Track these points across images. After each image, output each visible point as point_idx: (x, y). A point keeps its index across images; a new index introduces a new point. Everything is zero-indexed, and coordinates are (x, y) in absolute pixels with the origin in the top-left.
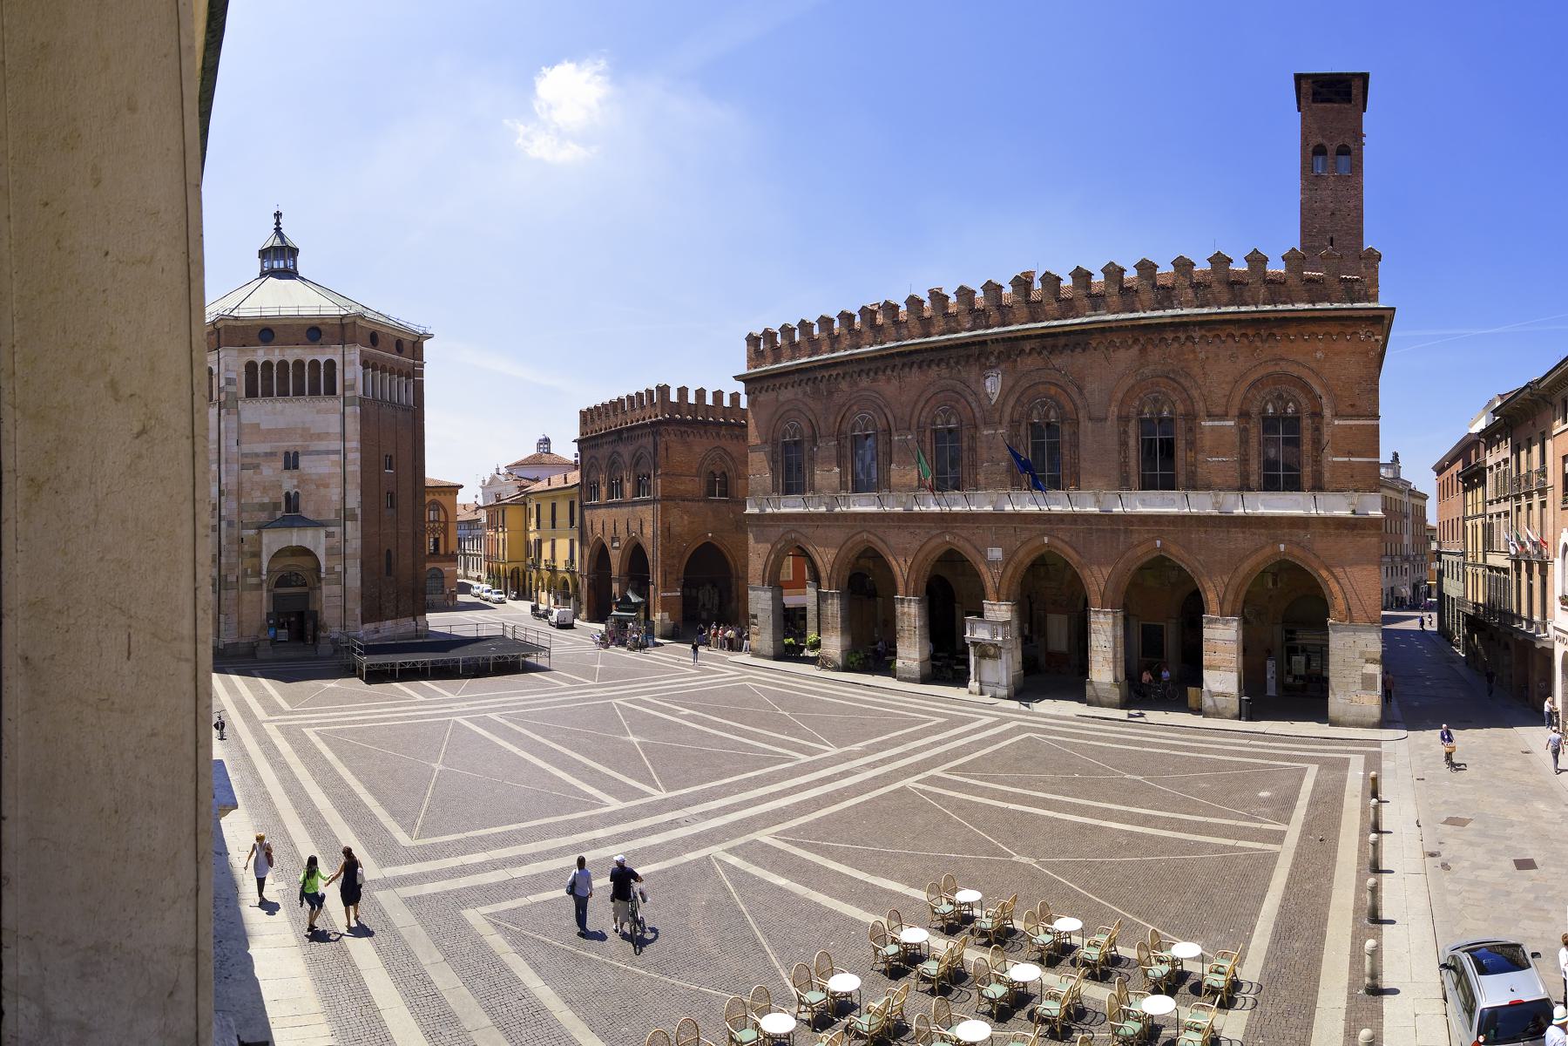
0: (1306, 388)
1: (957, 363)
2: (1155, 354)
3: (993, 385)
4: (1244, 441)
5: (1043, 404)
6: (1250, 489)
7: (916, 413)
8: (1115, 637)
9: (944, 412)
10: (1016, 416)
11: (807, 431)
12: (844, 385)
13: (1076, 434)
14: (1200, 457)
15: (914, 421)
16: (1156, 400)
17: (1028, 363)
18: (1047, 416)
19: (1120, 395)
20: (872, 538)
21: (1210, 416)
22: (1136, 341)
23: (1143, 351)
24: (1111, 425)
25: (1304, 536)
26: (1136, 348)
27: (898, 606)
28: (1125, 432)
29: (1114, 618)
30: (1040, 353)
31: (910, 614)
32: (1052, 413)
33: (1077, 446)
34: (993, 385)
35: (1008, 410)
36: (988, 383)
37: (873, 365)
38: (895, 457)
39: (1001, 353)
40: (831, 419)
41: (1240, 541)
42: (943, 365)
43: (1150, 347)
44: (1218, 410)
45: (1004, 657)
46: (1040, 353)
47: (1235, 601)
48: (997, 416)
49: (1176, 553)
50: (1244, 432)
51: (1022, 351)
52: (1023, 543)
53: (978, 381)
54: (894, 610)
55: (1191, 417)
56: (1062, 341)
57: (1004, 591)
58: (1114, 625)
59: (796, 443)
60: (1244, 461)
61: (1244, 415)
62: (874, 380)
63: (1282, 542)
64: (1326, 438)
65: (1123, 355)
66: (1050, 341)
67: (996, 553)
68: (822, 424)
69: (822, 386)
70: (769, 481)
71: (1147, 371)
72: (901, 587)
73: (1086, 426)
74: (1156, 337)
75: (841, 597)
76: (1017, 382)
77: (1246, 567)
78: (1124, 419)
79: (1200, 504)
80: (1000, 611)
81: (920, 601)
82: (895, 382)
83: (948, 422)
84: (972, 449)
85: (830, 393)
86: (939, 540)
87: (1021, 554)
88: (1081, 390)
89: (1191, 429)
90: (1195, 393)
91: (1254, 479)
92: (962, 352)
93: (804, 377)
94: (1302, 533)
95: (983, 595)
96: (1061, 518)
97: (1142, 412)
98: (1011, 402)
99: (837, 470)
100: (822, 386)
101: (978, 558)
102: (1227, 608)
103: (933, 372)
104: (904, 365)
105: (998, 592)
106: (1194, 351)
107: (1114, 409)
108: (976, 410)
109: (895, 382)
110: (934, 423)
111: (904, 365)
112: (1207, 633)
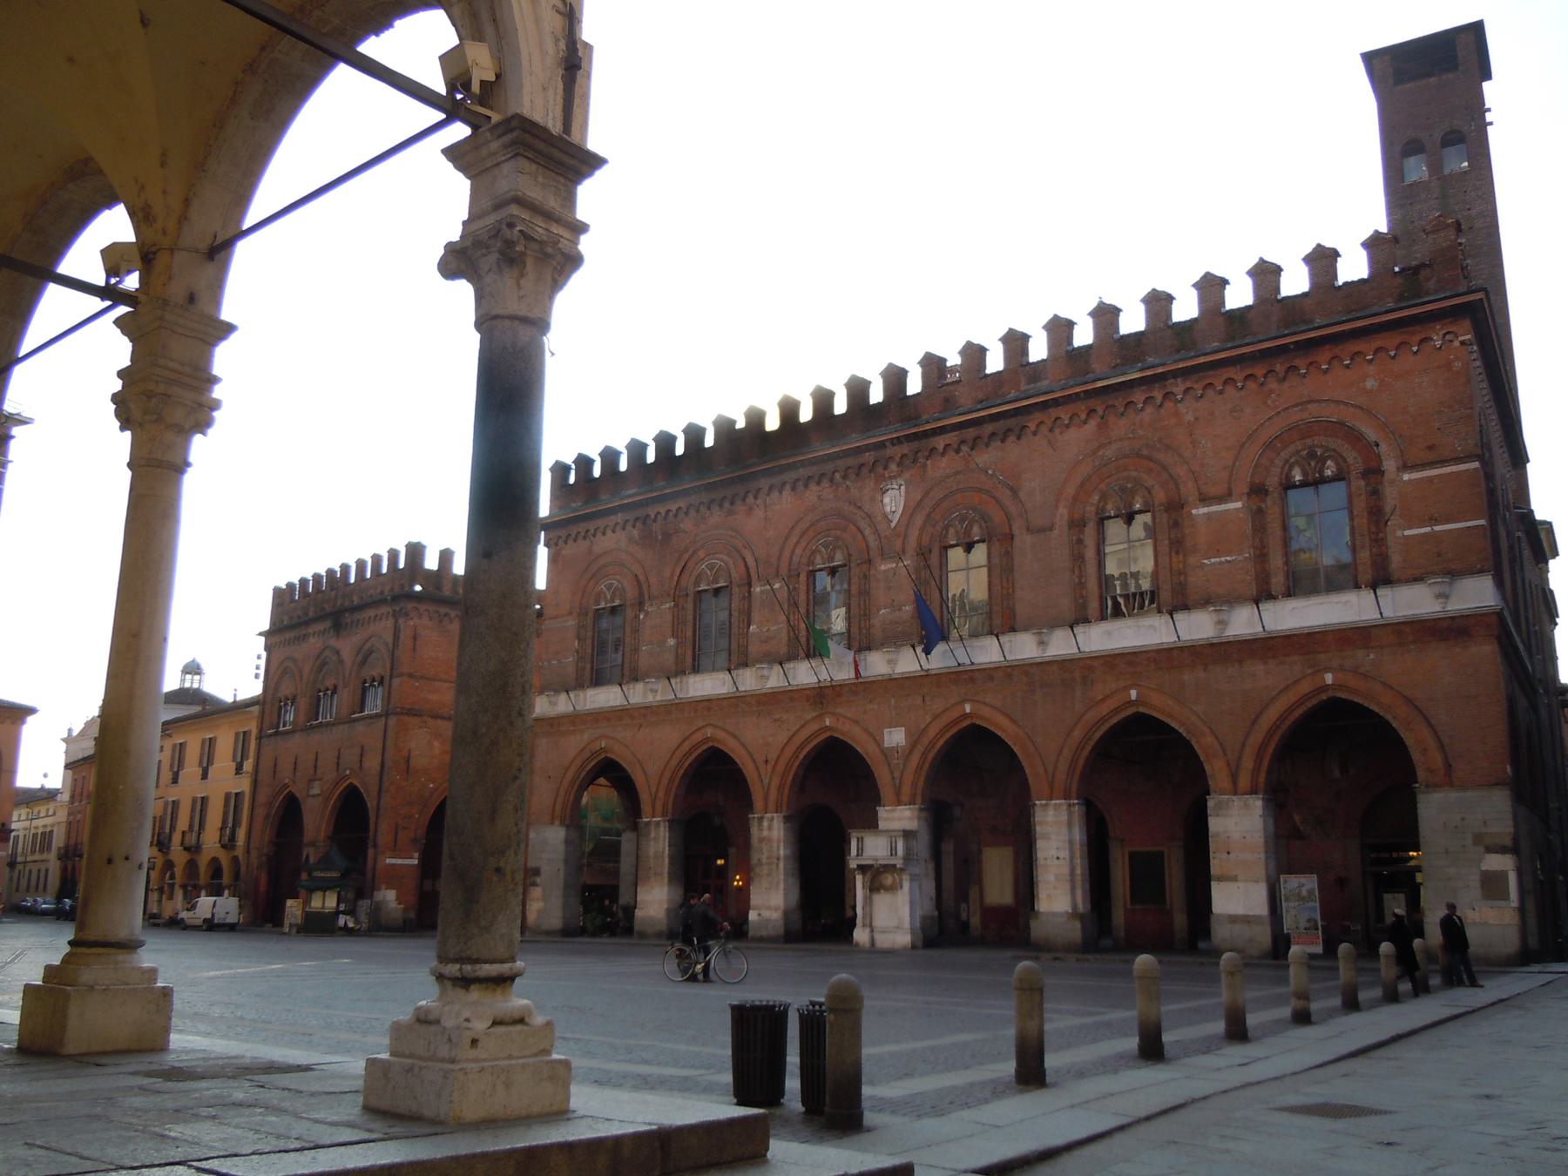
0: (1355, 437)
1: (845, 477)
2: (1120, 426)
3: (893, 501)
4: (1260, 528)
5: (962, 519)
6: (1271, 597)
7: (787, 554)
8: (1071, 842)
9: (826, 546)
10: (926, 540)
11: (631, 593)
13: (1008, 554)
14: (1192, 560)
16: (1123, 489)
17: (942, 466)
18: (968, 532)
19: (1070, 490)
20: (721, 735)
21: (1205, 499)
22: (1091, 412)
23: (1103, 425)
25: (1366, 658)
26: (1092, 425)
27: (754, 831)
28: (1080, 541)
29: (1070, 813)
30: (958, 451)
31: (771, 835)
32: (976, 529)
33: (1012, 570)
34: (893, 501)
35: (914, 534)
36: (887, 500)
38: (756, 616)
39: (903, 456)
41: (1262, 676)
42: (825, 483)
43: (1111, 419)
44: (1212, 490)
45: (906, 885)
46: (958, 451)
47: (1256, 769)
48: (899, 542)
49: (1163, 706)
50: (1259, 514)
51: (933, 449)
52: (935, 717)
53: (873, 499)
55: (1176, 506)
56: (989, 428)
57: (906, 790)
58: (1070, 825)
59: (614, 610)
60: (1261, 556)
61: (1257, 491)
62: (731, 513)
63: (1327, 670)
64: (1388, 509)
65: (1073, 434)
66: (971, 433)
67: (896, 737)
68: (653, 580)
70: (571, 670)
71: (1109, 453)
72: (758, 803)
73: (1024, 541)
74: (1119, 403)
75: (672, 823)
76: (926, 494)
77: (1272, 714)
78: (1077, 524)
79: (1197, 626)
80: (899, 817)
81: (787, 819)
82: (759, 513)
83: (832, 559)
85: (667, 537)
86: (814, 727)
87: (931, 733)
88: (1014, 492)
89: (1176, 524)
90: (1181, 471)
91: (1278, 582)
92: (851, 461)
93: (630, 516)
94: (1360, 653)
95: (877, 800)
96: (989, 674)
97: (1103, 509)
98: (919, 520)
99: (672, 642)
102: (1244, 781)
103: (812, 494)
104: (771, 487)
105: (898, 794)
106: (1177, 414)
107: (1063, 512)
110: (811, 562)
111: (771, 487)
112: (1215, 824)
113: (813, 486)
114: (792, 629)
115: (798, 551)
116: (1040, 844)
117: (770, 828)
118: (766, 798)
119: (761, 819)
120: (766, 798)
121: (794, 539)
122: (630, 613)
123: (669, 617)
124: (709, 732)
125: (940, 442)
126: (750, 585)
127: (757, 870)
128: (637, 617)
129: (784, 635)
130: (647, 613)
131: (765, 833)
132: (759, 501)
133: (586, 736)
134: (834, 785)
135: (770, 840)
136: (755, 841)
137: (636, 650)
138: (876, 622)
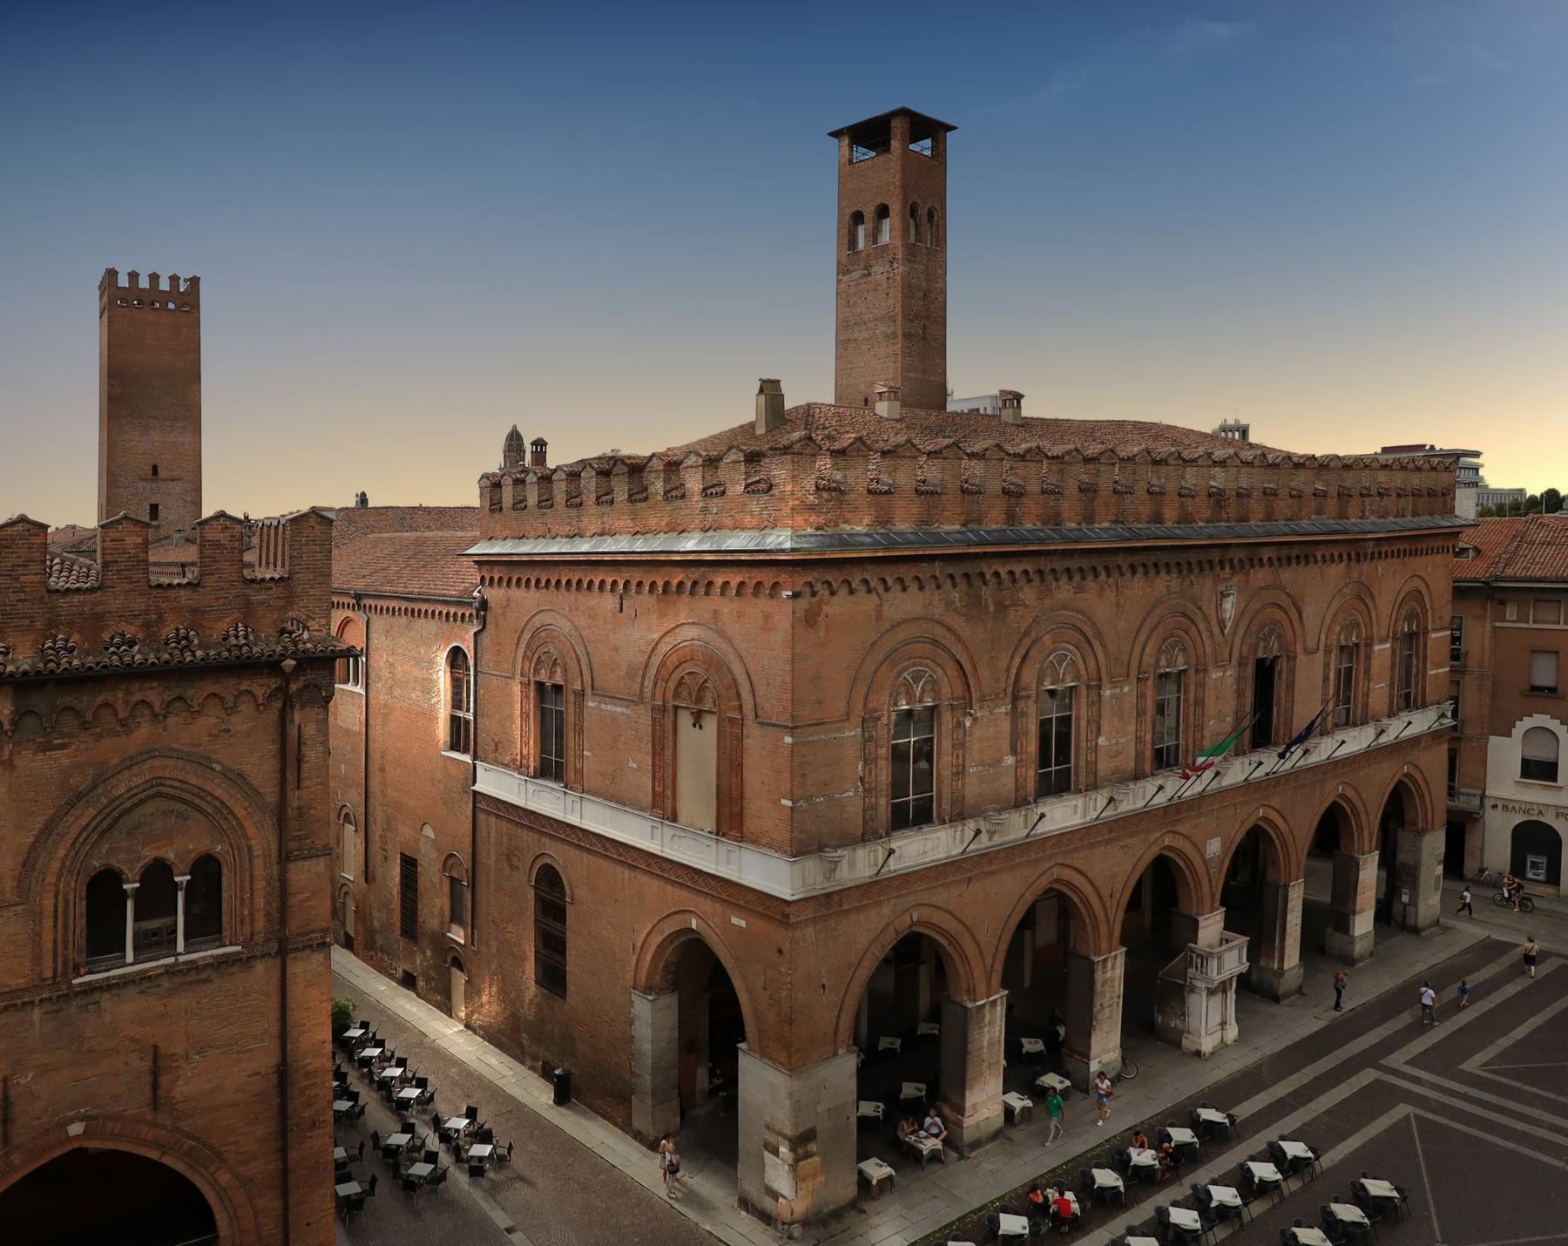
10: (1245, 651)
12: (1028, 594)
15: (1134, 664)
17: (1260, 576)
20: (1068, 874)
23: (1348, 567)
24: (1320, 655)
27: (1099, 976)
35: (1238, 642)
37: (1085, 563)
40: (1003, 664)
53: (1210, 601)
54: (1092, 981)
56: (1295, 551)
61: (1395, 638)
62: (1079, 589)
66: (1285, 552)
67: (1214, 847)
69: (987, 593)
73: (1301, 659)
82: (1110, 595)
84: (1200, 702)
85: (1002, 608)
98: (1241, 632)
99: (1010, 760)
100: (987, 593)
101: (1197, 862)
108: (1207, 643)
109: (1110, 595)
113: (1163, 574)
114: (1139, 740)
115: (1148, 650)
116: (1289, 917)
117: (1113, 967)
118: (1111, 934)
119: (1105, 961)
120: (1111, 934)
121: (1143, 637)
122: (947, 719)
123: (1006, 726)
124: (1056, 873)
125: (1266, 554)
126: (1100, 688)
127: (1099, 1017)
128: (960, 725)
129: (1133, 744)
130: (976, 720)
131: (1109, 974)
132: (1111, 580)
133: (886, 910)
134: (1159, 904)
135: (1113, 980)
136: (1098, 987)
137: (960, 773)
138: (1207, 733)
